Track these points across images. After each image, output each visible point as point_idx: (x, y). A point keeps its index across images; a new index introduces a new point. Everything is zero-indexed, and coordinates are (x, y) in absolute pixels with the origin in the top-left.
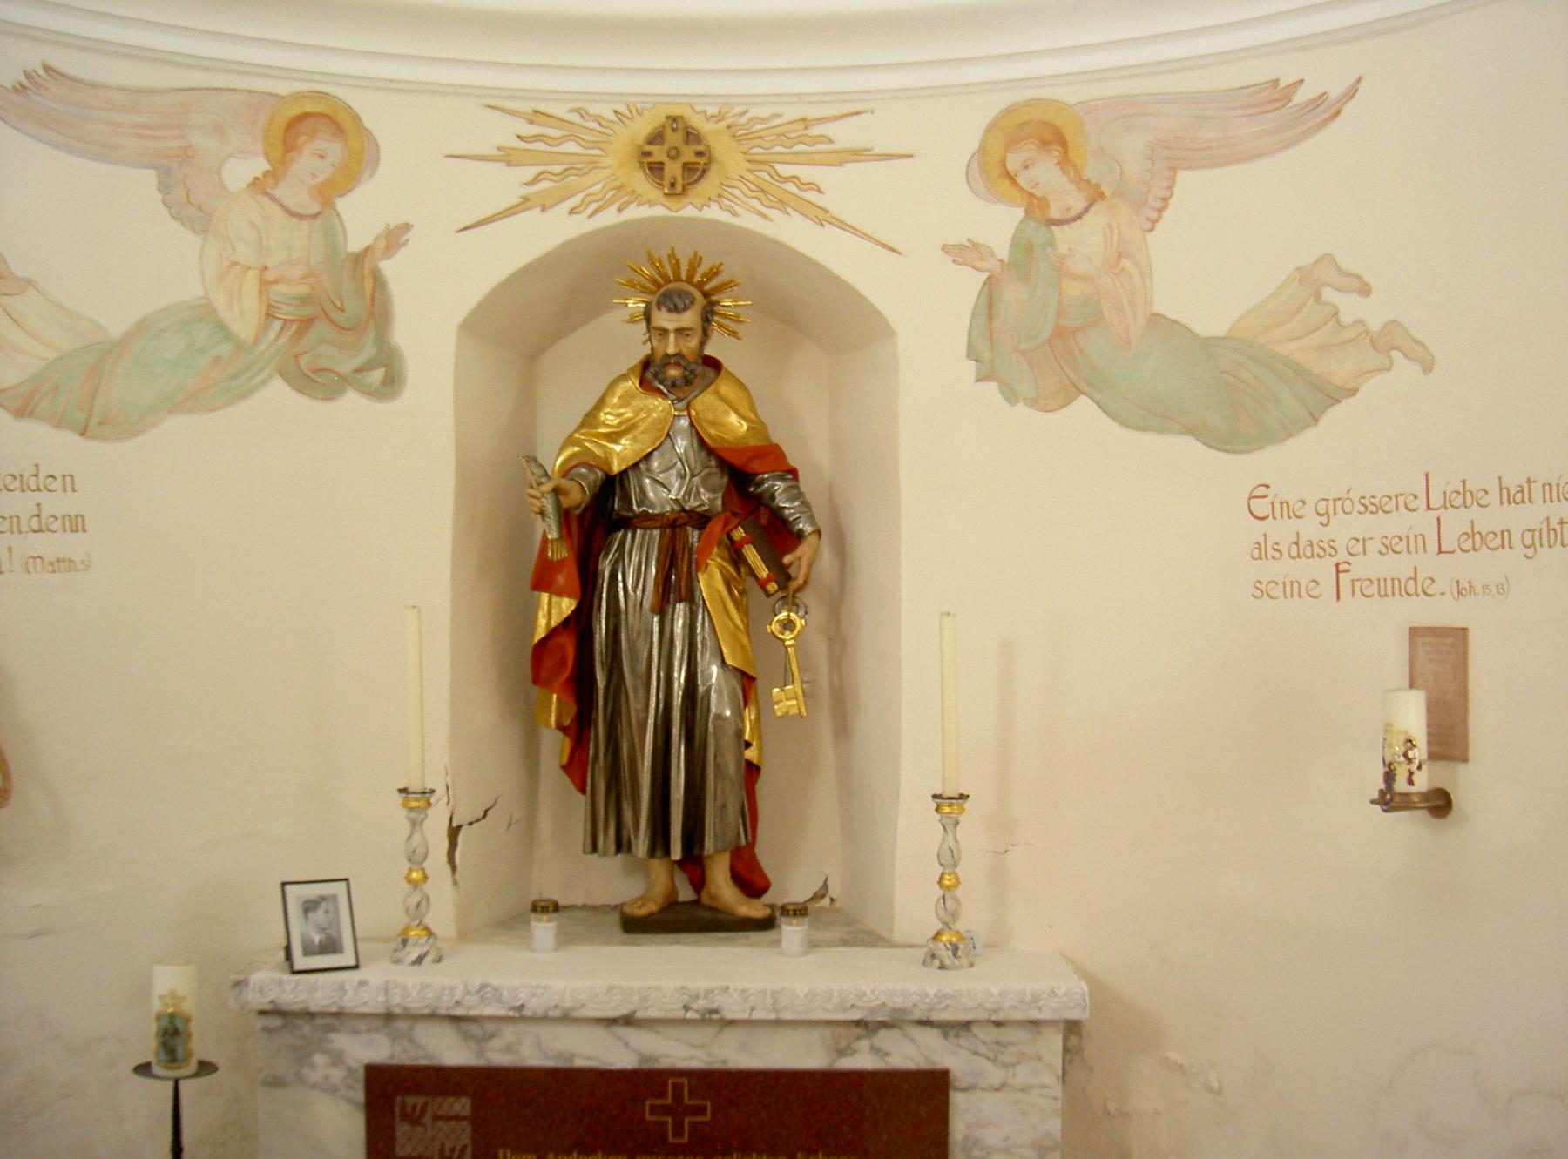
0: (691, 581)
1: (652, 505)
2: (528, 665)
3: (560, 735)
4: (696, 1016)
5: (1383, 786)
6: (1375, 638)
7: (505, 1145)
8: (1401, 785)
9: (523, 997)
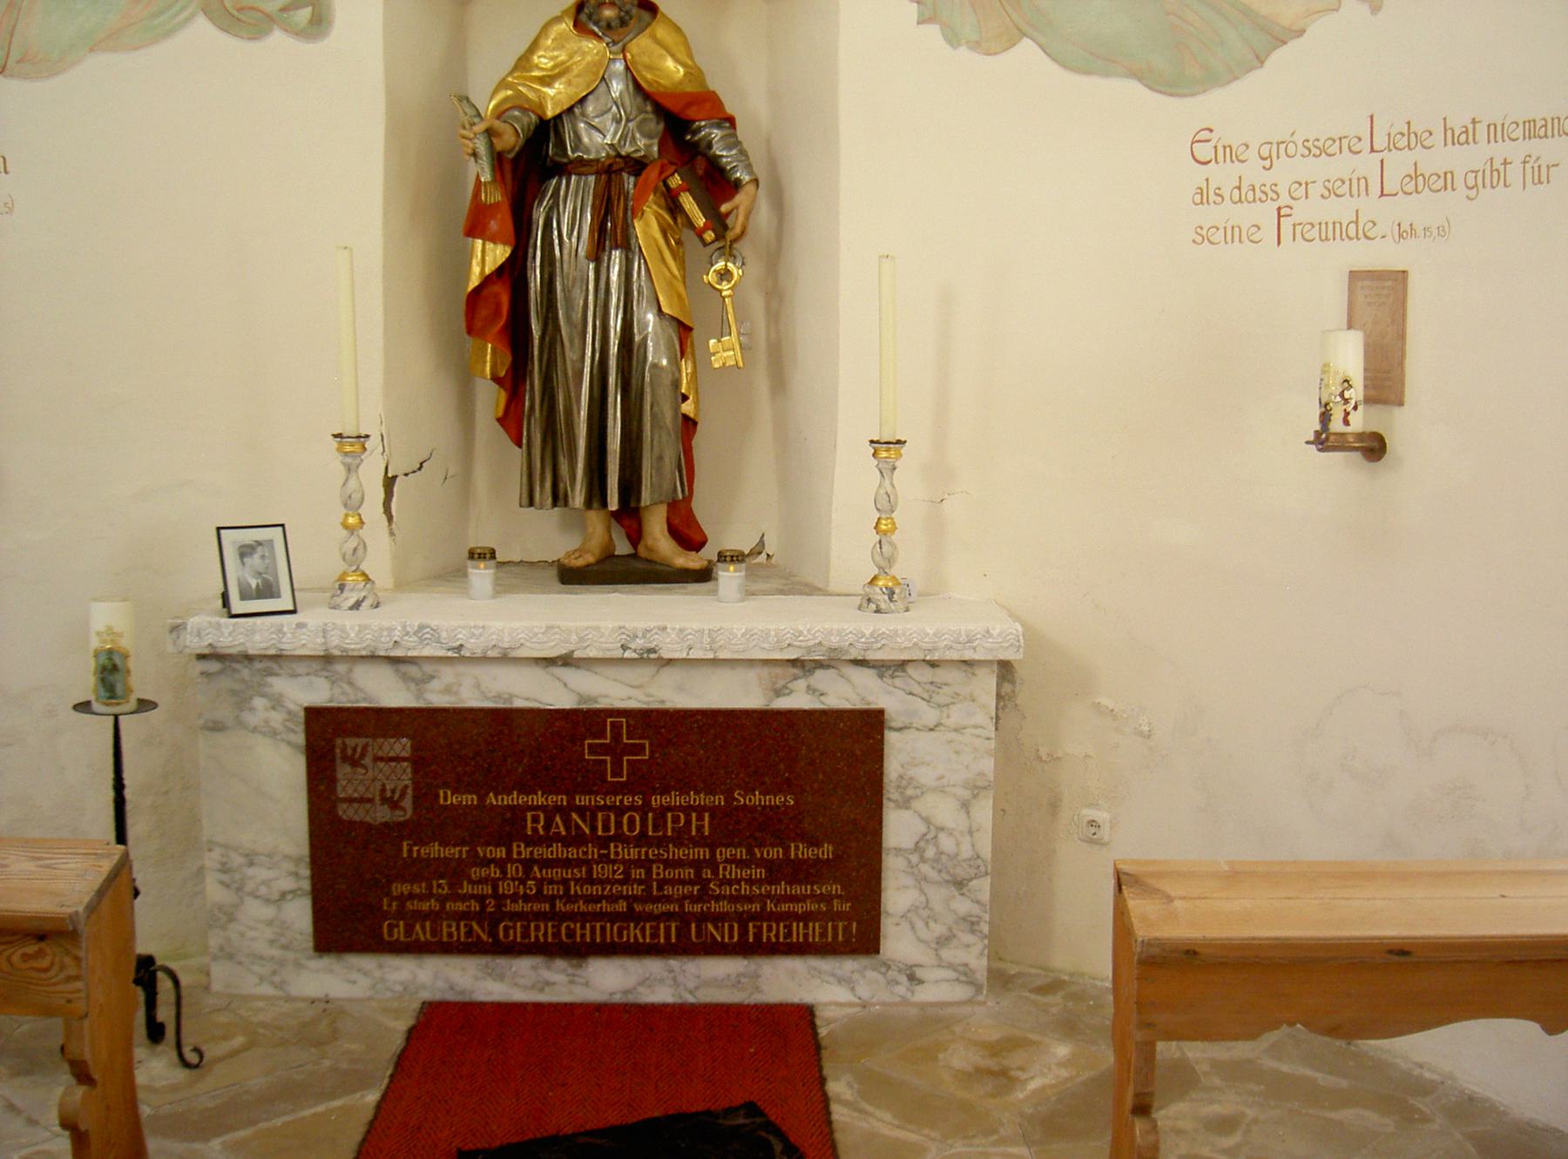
0: (627, 229)
1: (587, 151)
2: (463, 307)
3: (495, 387)
4: (635, 655)
5: (1318, 428)
6: (1314, 281)
7: (446, 785)
8: (1336, 425)
9: (462, 637)
